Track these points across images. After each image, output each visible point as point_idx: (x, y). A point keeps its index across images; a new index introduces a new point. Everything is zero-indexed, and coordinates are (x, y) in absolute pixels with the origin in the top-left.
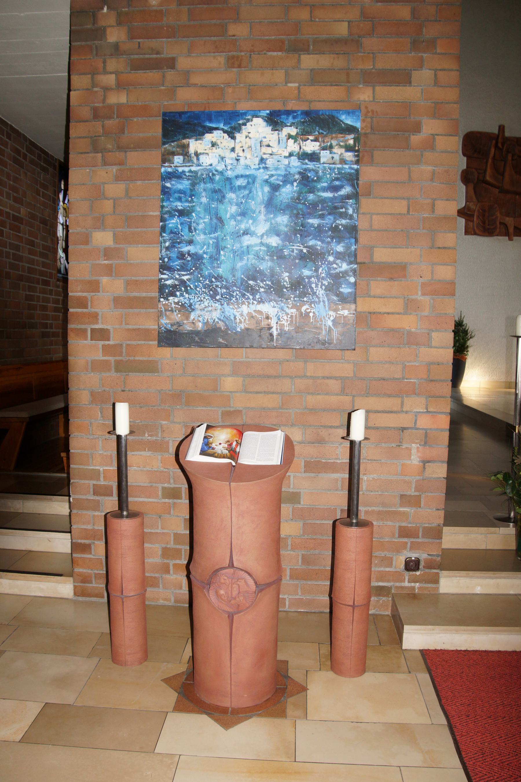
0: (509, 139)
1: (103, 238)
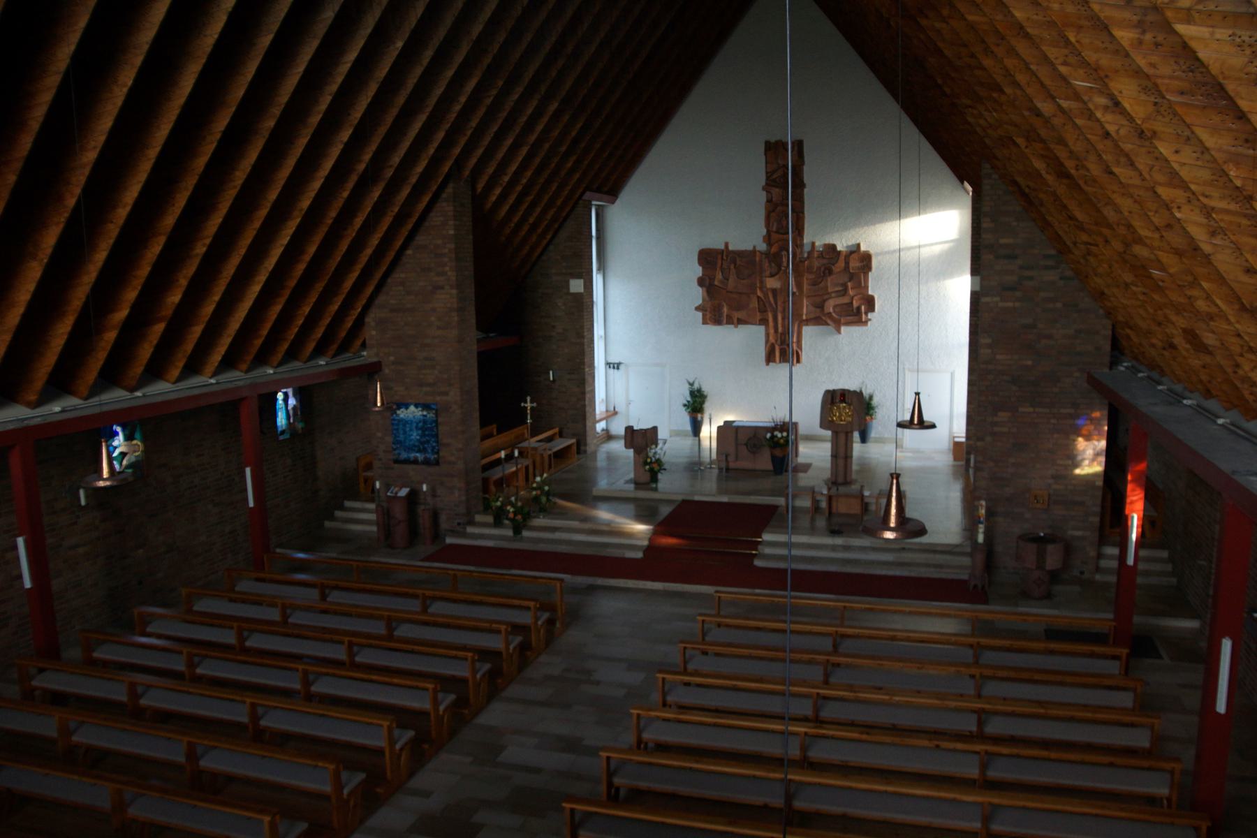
0: (733, 252)
1: (379, 435)
